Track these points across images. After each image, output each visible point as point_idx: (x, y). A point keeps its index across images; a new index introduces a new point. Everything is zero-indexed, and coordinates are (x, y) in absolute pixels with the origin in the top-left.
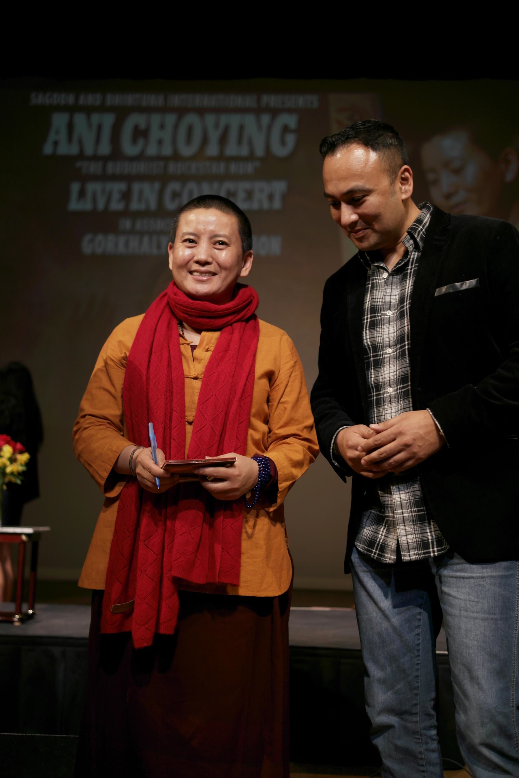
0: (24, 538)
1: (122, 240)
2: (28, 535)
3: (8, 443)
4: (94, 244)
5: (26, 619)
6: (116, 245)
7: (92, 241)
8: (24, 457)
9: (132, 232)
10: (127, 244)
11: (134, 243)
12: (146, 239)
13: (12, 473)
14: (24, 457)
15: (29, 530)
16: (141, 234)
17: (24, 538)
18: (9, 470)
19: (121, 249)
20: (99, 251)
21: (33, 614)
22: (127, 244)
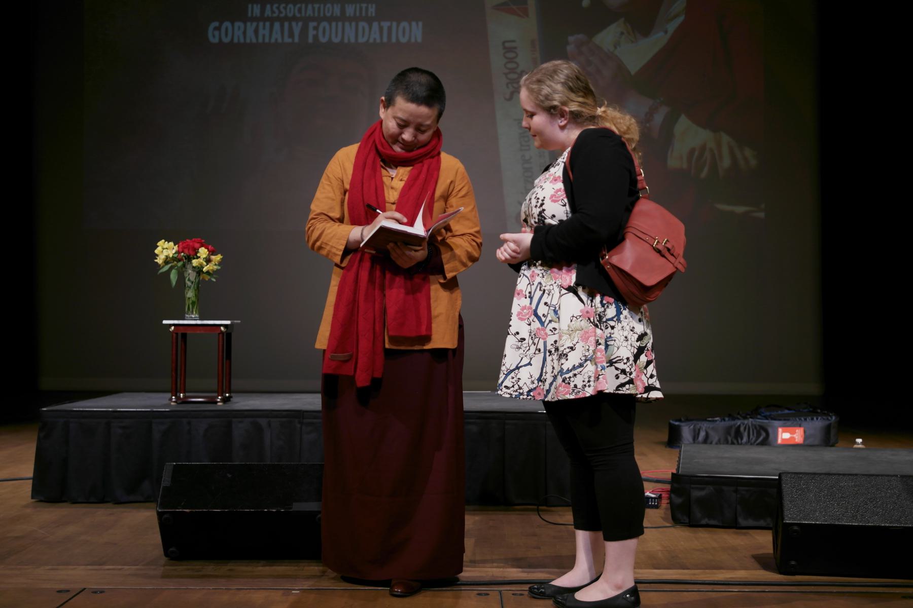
0: (222, 328)
1: (251, 27)
2: (225, 326)
3: (202, 246)
4: (221, 32)
5: (226, 400)
6: (244, 33)
7: (218, 29)
8: (217, 258)
9: (262, 18)
10: (256, 31)
11: (264, 31)
12: (277, 25)
13: (208, 272)
14: (217, 258)
15: (228, 322)
16: (272, 20)
17: (222, 328)
18: (205, 269)
19: (251, 37)
20: (226, 40)
21: (230, 397)
22: (256, 31)
